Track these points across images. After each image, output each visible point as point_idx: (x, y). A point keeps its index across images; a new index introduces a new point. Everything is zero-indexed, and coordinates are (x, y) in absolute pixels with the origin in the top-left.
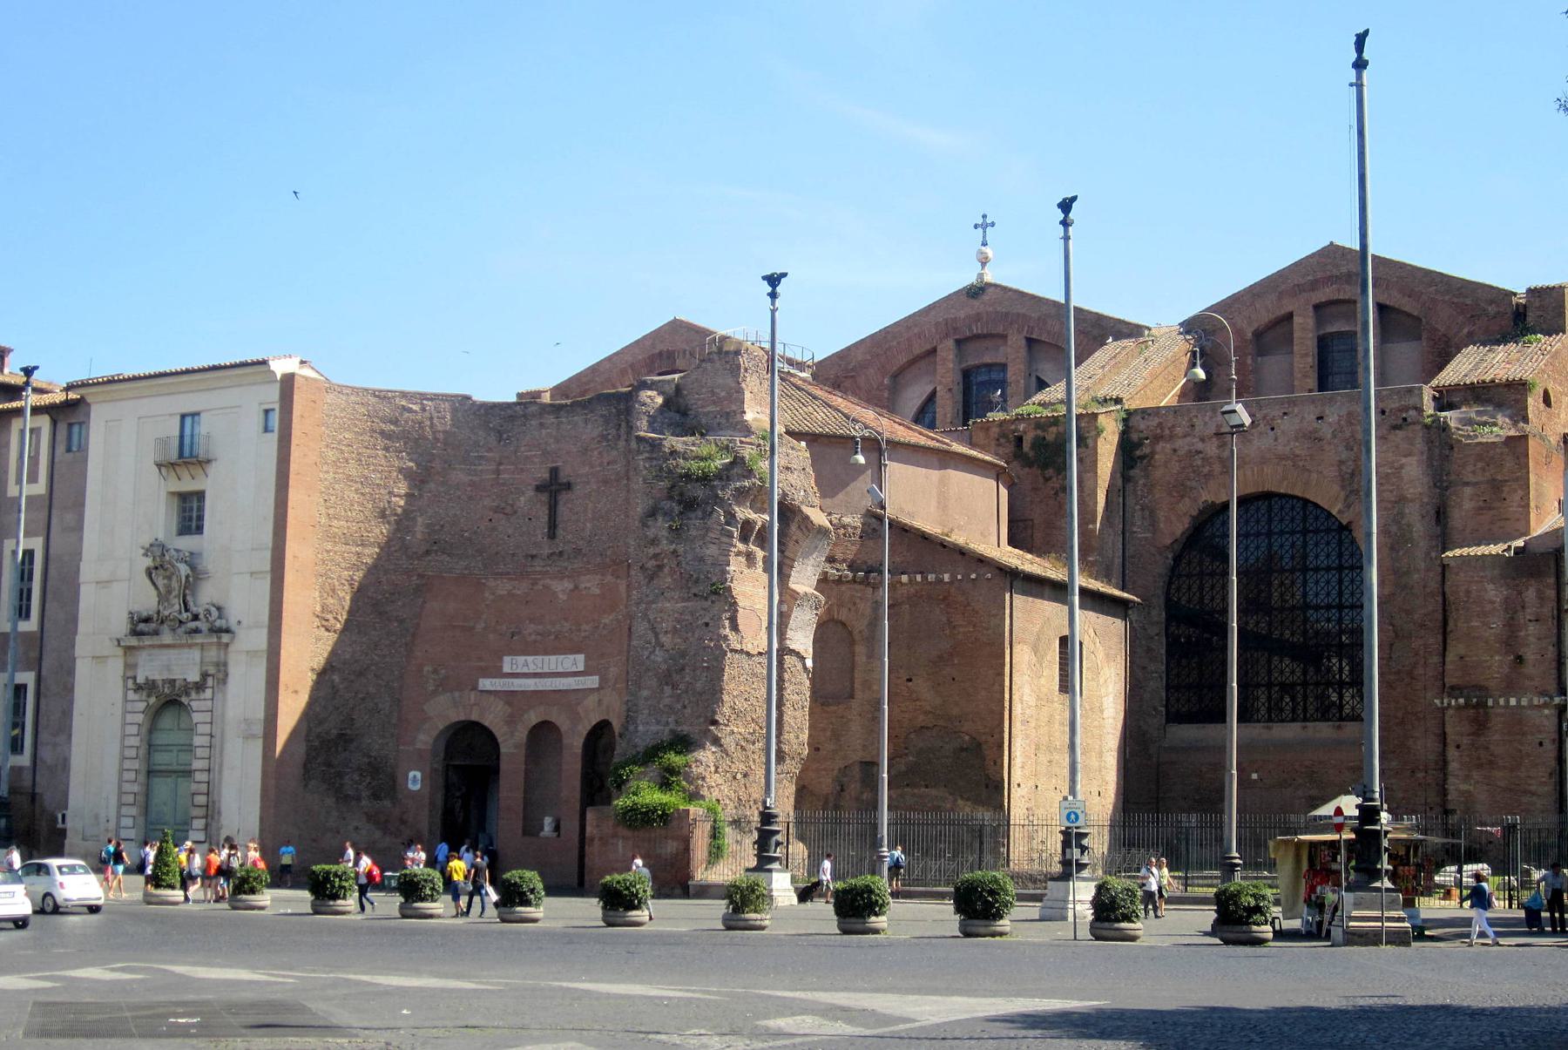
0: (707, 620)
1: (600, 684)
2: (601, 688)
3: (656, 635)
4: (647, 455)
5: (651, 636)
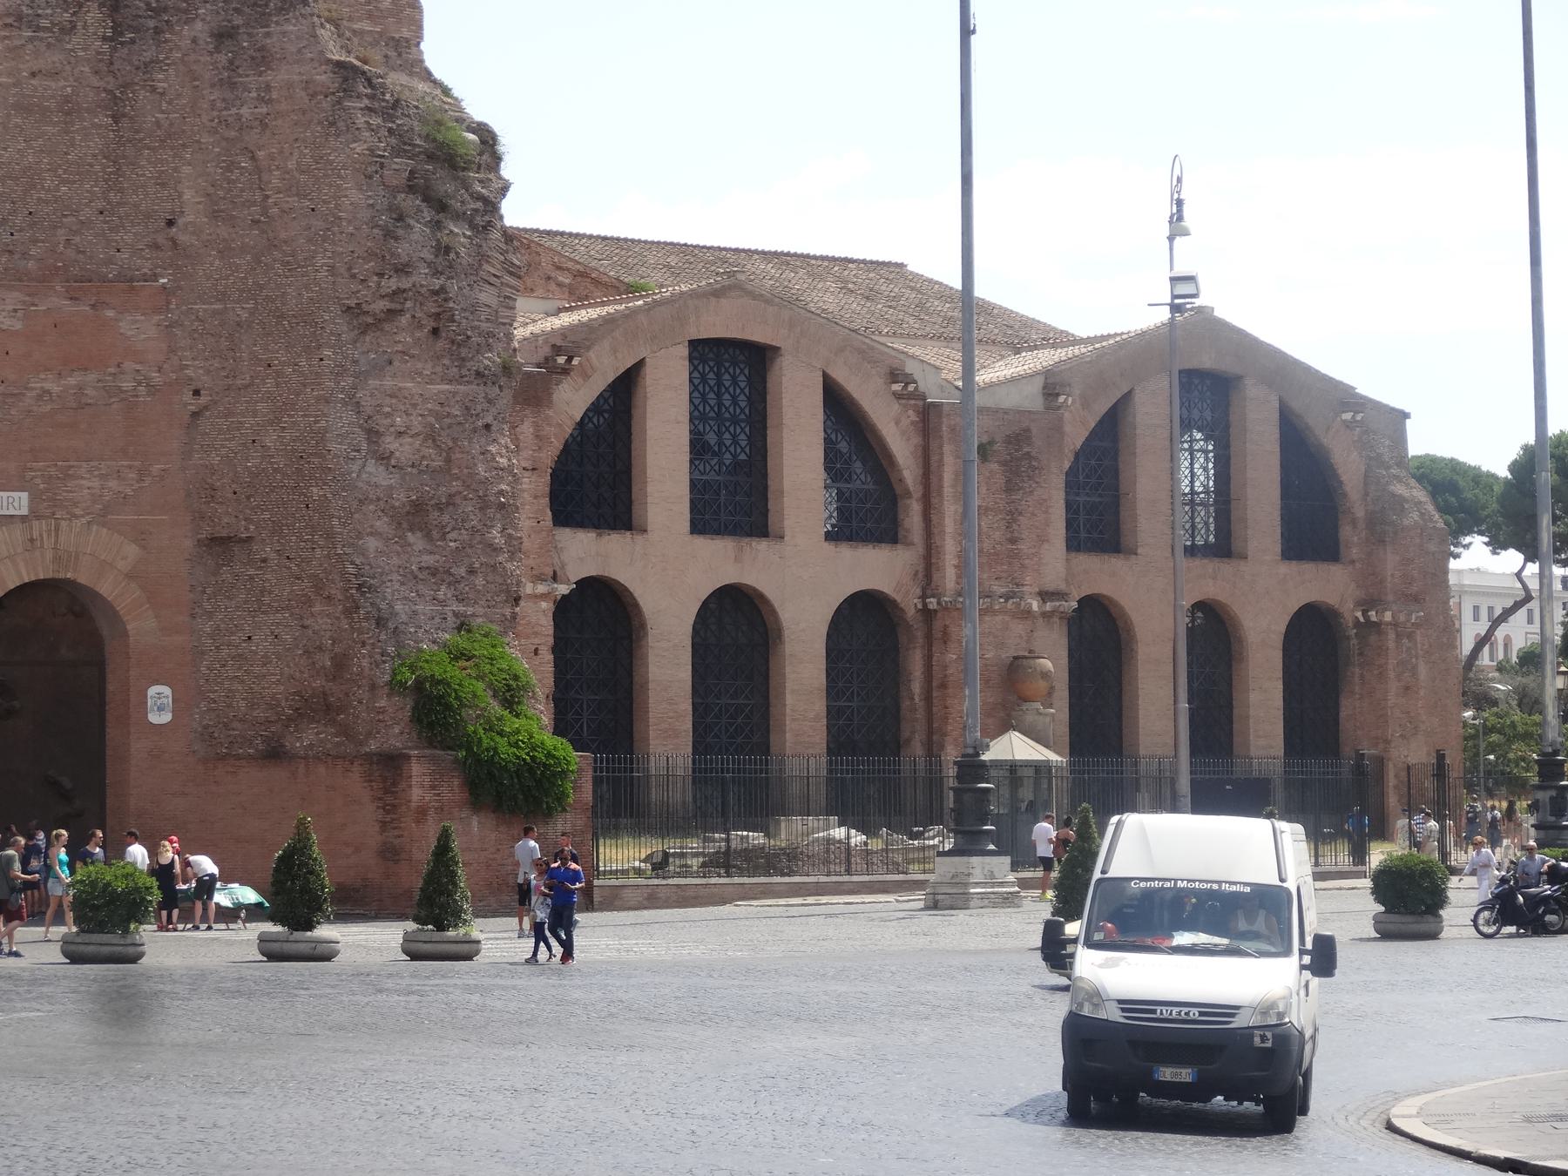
0: (489, 419)
1: (31, 510)
2: (34, 514)
3: (373, 435)
4: (366, 102)
5: (360, 438)
